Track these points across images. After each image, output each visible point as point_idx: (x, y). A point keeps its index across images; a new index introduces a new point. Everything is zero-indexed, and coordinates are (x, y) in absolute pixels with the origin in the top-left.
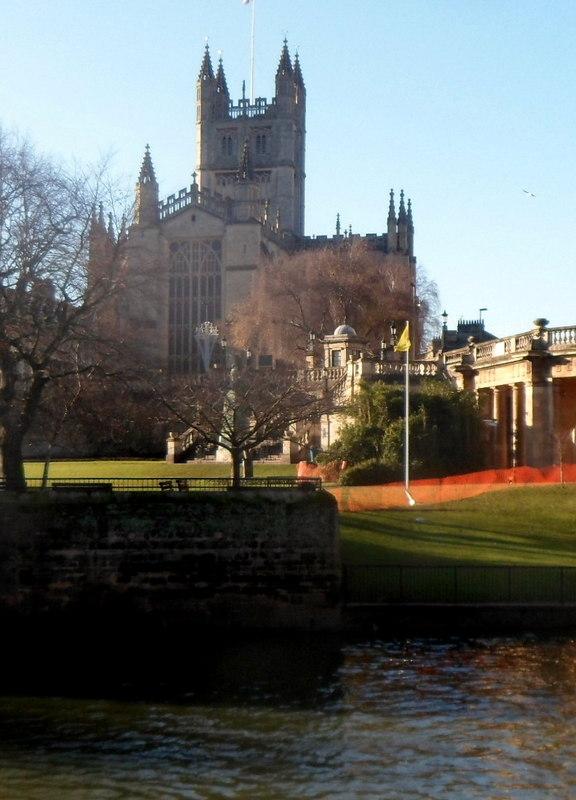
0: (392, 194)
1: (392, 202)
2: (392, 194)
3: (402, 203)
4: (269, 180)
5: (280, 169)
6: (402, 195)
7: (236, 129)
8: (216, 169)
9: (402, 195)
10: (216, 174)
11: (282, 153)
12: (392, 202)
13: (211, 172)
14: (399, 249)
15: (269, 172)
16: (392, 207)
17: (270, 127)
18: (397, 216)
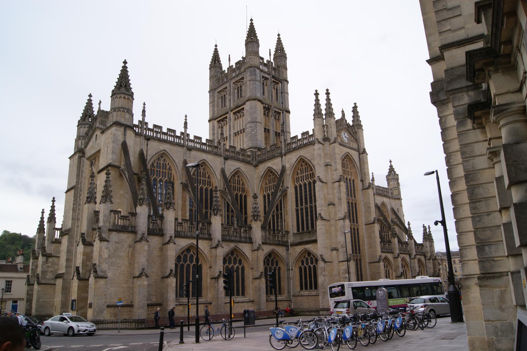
0: (317, 94)
1: (317, 100)
2: (317, 94)
3: (328, 99)
4: (244, 115)
5: (248, 103)
6: (328, 93)
7: (226, 88)
8: (217, 118)
9: (328, 93)
10: (218, 122)
11: (248, 92)
12: (317, 100)
13: (214, 121)
14: (326, 139)
15: (243, 109)
16: (317, 104)
17: (243, 78)
18: (324, 112)
